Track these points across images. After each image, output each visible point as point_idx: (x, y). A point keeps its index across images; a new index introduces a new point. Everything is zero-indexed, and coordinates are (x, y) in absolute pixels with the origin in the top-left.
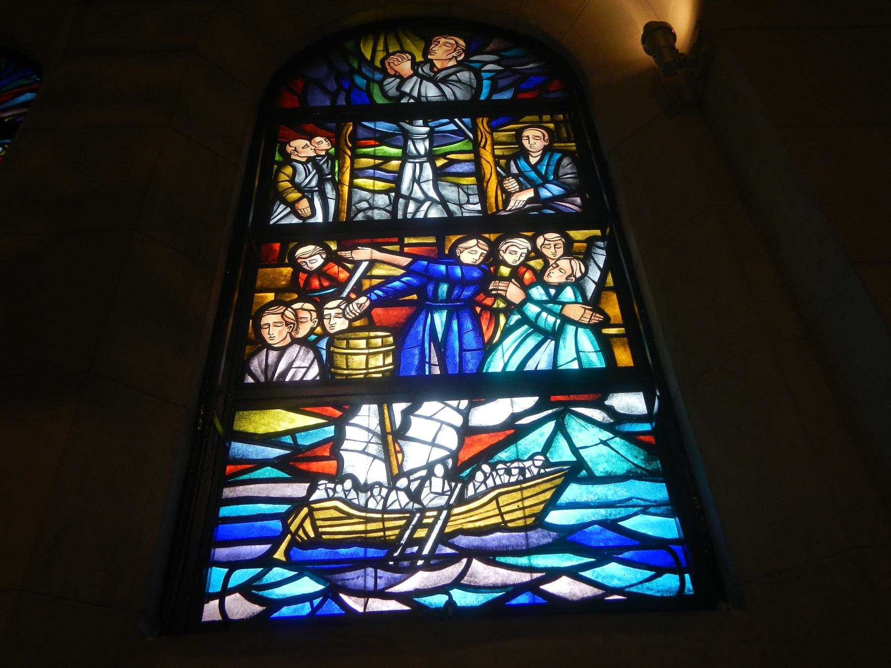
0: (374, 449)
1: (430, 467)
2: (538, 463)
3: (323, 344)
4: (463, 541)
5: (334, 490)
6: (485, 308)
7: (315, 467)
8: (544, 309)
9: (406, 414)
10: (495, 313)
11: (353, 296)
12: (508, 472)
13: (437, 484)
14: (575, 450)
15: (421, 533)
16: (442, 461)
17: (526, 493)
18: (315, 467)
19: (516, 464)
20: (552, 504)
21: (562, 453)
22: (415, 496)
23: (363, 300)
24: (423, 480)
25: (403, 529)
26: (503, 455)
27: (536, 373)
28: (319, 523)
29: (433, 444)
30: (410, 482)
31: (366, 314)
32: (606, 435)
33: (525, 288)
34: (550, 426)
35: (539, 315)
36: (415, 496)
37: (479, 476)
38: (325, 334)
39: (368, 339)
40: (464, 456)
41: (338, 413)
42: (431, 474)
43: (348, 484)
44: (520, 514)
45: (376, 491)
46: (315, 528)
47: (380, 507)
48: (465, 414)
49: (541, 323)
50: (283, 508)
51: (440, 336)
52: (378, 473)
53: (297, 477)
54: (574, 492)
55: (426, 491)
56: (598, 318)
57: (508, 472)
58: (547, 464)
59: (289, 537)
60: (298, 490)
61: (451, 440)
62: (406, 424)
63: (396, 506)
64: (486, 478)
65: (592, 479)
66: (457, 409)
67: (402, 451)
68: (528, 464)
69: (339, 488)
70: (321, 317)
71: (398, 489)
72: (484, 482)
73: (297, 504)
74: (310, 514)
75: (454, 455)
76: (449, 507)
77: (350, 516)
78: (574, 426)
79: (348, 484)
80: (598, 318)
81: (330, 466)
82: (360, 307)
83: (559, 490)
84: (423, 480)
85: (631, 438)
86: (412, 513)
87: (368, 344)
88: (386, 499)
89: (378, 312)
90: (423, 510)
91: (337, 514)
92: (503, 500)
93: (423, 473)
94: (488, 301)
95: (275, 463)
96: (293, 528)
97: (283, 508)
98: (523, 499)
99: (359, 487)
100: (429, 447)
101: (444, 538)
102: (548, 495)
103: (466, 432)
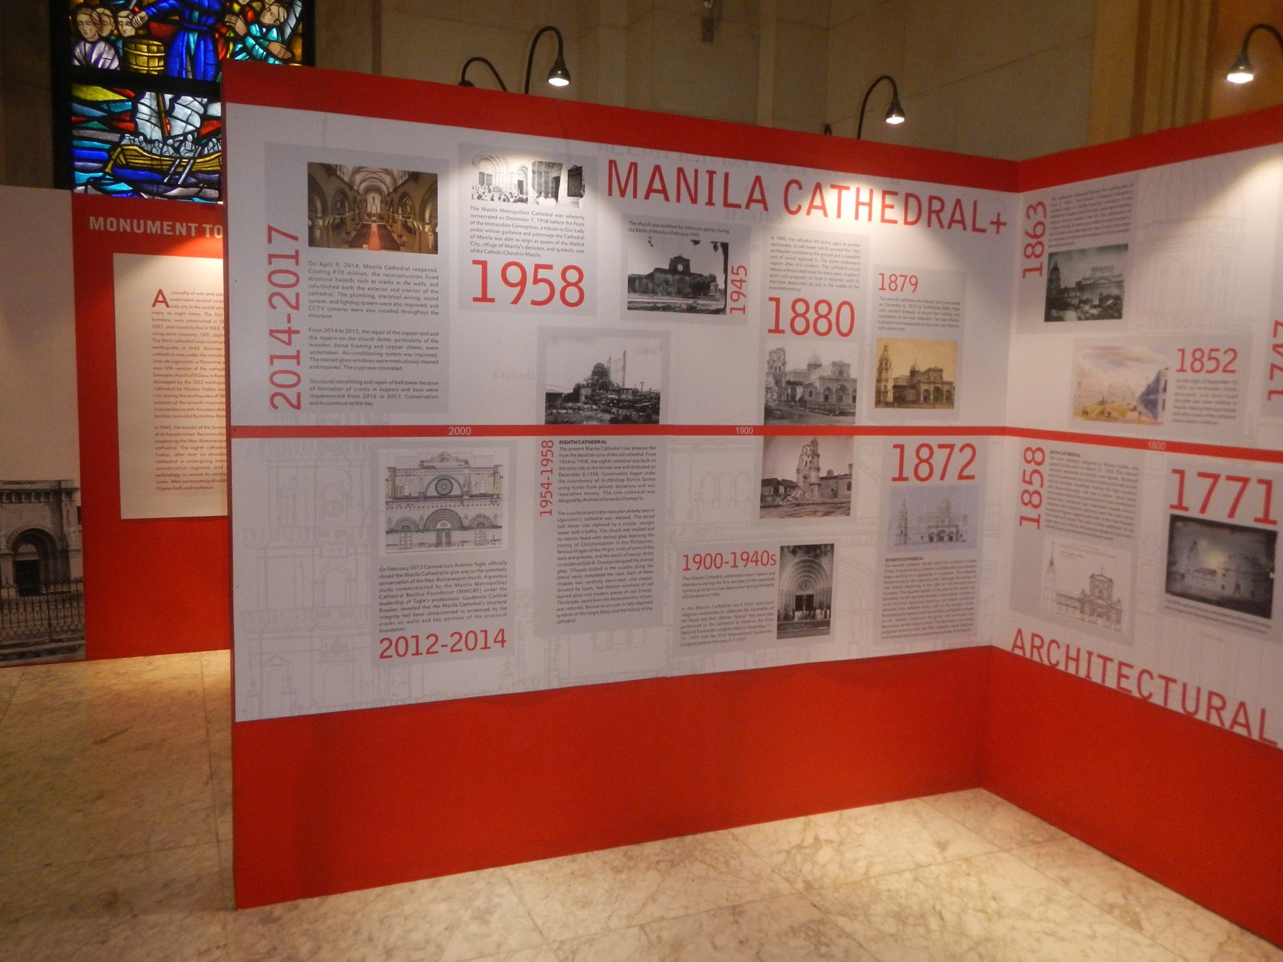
0: (153, 120)
1: (185, 135)
3: (120, 44)
4: (201, 176)
5: (134, 140)
6: (222, 35)
7: (123, 125)
8: (257, 43)
9: (173, 101)
10: (228, 40)
11: (137, 10)
13: (189, 145)
15: (180, 169)
16: (191, 133)
18: (123, 125)
22: (177, 150)
23: (143, 14)
24: (182, 142)
25: (171, 166)
29: (187, 122)
30: (174, 142)
31: (145, 26)
33: (248, 24)
35: (254, 46)
36: (177, 150)
37: (211, 144)
38: (120, 36)
39: (149, 45)
40: (204, 131)
41: (133, 94)
42: (185, 139)
43: (141, 138)
45: (156, 144)
47: (159, 153)
48: (205, 107)
49: (254, 53)
50: (107, 146)
51: (193, 52)
52: (156, 134)
55: (182, 149)
56: (289, 55)
59: (112, 162)
60: (114, 137)
61: (197, 121)
62: (172, 108)
63: (167, 154)
64: (214, 146)
66: (200, 103)
67: (169, 123)
69: (136, 139)
70: (117, 22)
71: (168, 145)
72: (213, 148)
73: (115, 145)
75: (197, 130)
76: (194, 158)
77: (145, 156)
79: (141, 138)
80: (289, 55)
82: (142, 18)
84: (182, 142)
86: (176, 158)
87: (148, 49)
88: (162, 149)
89: (154, 25)
90: (181, 158)
93: (182, 138)
94: (224, 30)
95: (99, 119)
96: (114, 157)
97: (107, 146)
99: (150, 141)
100: (184, 124)
101: (191, 174)
103: (205, 118)
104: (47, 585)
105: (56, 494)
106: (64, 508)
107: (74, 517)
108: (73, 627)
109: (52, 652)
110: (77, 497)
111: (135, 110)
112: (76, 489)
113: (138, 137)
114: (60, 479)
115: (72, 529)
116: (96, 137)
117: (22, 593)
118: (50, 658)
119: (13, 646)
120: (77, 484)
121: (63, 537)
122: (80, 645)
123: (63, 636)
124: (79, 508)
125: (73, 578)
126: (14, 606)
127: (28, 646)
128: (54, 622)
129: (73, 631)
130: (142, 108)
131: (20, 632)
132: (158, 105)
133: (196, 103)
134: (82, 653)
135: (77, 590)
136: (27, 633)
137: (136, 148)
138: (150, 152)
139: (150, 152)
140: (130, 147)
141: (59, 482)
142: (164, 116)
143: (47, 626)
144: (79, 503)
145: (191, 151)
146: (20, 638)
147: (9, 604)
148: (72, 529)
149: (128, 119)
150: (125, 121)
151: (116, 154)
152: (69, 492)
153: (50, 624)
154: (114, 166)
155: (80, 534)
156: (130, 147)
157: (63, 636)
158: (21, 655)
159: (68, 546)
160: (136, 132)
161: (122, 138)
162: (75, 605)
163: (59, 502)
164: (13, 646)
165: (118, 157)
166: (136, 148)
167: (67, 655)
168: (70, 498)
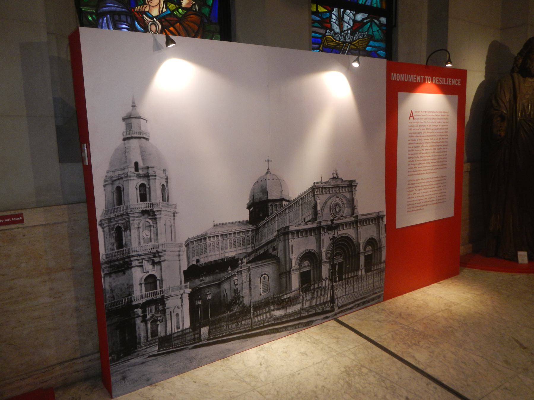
1: (347, 30)
2: (366, 34)
5: (330, 33)
9: (344, 12)
12: (361, 35)
13: (349, 35)
14: (373, 32)
16: (350, 29)
17: (364, 41)
19: (362, 33)
20: (367, 46)
21: (370, 33)
22: (345, 38)
26: (360, 30)
27: (367, 6)
28: (328, 42)
29: (348, 24)
30: (344, 34)
32: (378, 29)
34: (369, 24)
36: (345, 38)
37: (356, 35)
42: (348, 33)
43: (333, 31)
44: (362, 47)
46: (327, 43)
48: (354, 15)
50: (320, 36)
52: (338, 30)
53: (323, 27)
54: (371, 43)
57: (361, 35)
58: (367, 35)
60: (322, 31)
61: (351, 23)
62: (343, 16)
63: (341, 40)
65: (375, 40)
66: (353, 14)
67: (342, 24)
68: (365, 34)
72: (357, 37)
74: (326, 39)
75: (352, 28)
78: (373, 25)
81: (328, 25)
83: (369, 42)
85: (382, 30)
88: (340, 37)
91: (331, 40)
92: (360, 42)
93: (346, 32)
95: (318, 22)
96: (323, 42)
97: (320, 36)
98: (363, 43)
99: (336, 33)
100: (347, 25)
102: (367, 43)
103: (355, 21)
104: (374, 265)
105: (378, 218)
106: (380, 226)
107: (383, 230)
108: (380, 286)
109: (373, 300)
110: (385, 219)
111: (331, 17)
112: (384, 216)
113: (332, 31)
114: (379, 211)
115: (383, 236)
116: (317, 31)
117: (366, 271)
118: (372, 303)
119: (362, 299)
120: (385, 213)
121: (380, 241)
122: (382, 294)
123: (377, 291)
124: (385, 225)
125: (382, 261)
126: (363, 279)
127: (366, 298)
128: (375, 284)
129: (380, 288)
130: (334, 17)
131: (364, 291)
132: (338, 15)
133: (351, 14)
134: (382, 298)
135: (383, 267)
136: (366, 291)
137: (331, 37)
138: (335, 39)
139: (335, 39)
140: (329, 37)
141: (379, 212)
142: (341, 20)
143: (372, 287)
144: (385, 223)
145: (349, 39)
146: (364, 295)
147: (361, 278)
148: (383, 236)
149: (328, 22)
150: (327, 23)
151: (324, 40)
152: (382, 217)
153: (373, 285)
154: (323, 46)
155: (385, 238)
156: (329, 37)
157: (377, 291)
158: (364, 303)
159: (381, 245)
160: (331, 29)
161: (326, 32)
162: (382, 274)
163: (379, 223)
164: (362, 299)
165: (324, 42)
166: (331, 37)
167: (378, 300)
168: (382, 220)
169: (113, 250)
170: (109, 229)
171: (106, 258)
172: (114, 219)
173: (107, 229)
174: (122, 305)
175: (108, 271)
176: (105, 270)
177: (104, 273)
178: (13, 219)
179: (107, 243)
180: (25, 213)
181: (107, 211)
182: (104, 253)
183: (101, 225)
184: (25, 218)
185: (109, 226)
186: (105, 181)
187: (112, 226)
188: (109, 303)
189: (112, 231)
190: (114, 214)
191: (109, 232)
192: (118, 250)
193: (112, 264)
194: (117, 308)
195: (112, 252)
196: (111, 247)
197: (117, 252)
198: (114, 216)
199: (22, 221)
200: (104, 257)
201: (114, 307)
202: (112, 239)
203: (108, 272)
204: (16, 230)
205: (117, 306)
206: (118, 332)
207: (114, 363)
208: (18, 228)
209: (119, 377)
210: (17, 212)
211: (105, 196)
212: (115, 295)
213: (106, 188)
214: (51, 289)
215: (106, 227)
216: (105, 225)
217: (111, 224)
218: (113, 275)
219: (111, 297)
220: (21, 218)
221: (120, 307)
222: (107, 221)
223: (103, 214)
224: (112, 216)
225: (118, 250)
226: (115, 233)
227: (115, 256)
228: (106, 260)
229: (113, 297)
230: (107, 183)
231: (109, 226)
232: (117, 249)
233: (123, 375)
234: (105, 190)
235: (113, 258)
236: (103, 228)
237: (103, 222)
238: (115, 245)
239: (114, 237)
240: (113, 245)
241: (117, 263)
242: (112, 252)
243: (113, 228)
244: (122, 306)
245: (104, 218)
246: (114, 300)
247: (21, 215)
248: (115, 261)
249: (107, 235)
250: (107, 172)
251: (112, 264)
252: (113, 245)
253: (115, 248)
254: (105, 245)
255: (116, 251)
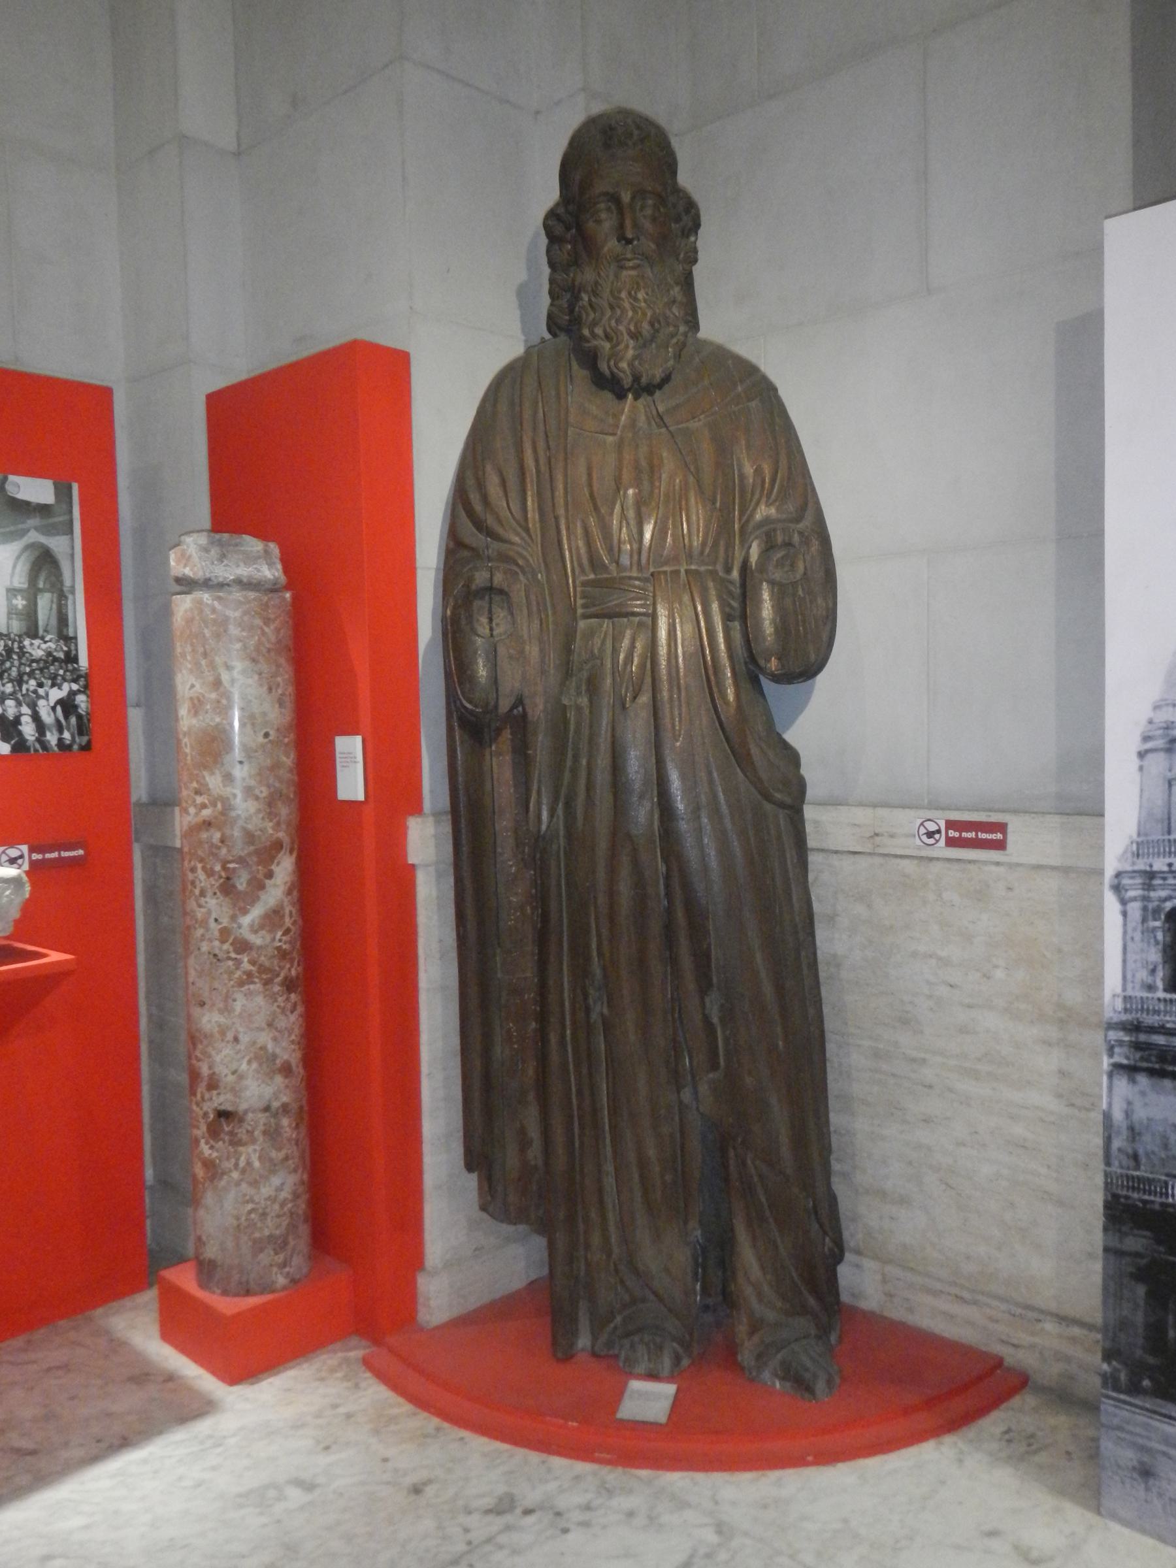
169: (1151, 988)
170: (1145, 909)
171: (1126, 1010)
172: (1164, 879)
173: (1135, 908)
174: (1164, 1200)
175: (1127, 1058)
176: (1117, 1050)
177: (1112, 1061)
178: (964, 835)
179: (1131, 957)
180: (1015, 825)
181: (1140, 848)
182: (1119, 990)
183: (1117, 888)
184: (1011, 838)
185: (1145, 899)
186: (1146, 738)
187: (1156, 903)
188: (1119, 1171)
189: (1155, 919)
190: (1168, 860)
191: (1144, 920)
192: (1168, 996)
193: (1143, 1037)
194: (1145, 1202)
195: (1145, 994)
196: (1143, 975)
197: (1165, 1000)
198: (1166, 869)
199: (1000, 845)
200: (1119, 1005)
201: (1135, 1195)
202: (1153, 950)
203: (1125, 1062)
204: (993, 868)
205: (1146, 1197)
206: (1141, 1290)
207: (1114, 1394)
208: (998, 864)
209: (1129, 1456)
210: (995, 818)
211: (1142, 790)
212: (1141, 1152)
213: (1145, 763)
214: (1062, 1073)
215: (1134, 899)
216: (1131, 893)
217: (1152, 894)
218: (1143, 1080)
219: (1128, 1156)
220: (999, 836)
221: (1157, 1207)
222: (1139, 881)
223: (1129, 855)
224: (1160, 865)
225: (1168, 996)
226: (1163, 928)
227: (1157, 1012)
228: (1124, 1017)
229: (1135, 1157)
230: (1149, 745)
231: (1145, 899)
232: (1165, 990)
233: (1146, 1458)
234: (1141, 768)
235: (1151, 1020)
236: (1123, 902)
237: (1126, 881)
238: (1160, 974)
239: (1157, 943)
240: (1153, 971)
241: (1160, 1040)
242: (1145, 994)
243: (1156, 912)
244: (1162, 1204)
245: (1129, 868)
246: (1137, 1168)
247: (1001, 827)
248: (1152, 1030)
249: (1135, 929)
250: (1156, 707)
251: (1143, 1037)
252: (1153, 971)
253: (1160, 984)
254: (1124, 961)
255: (1161, 994)
